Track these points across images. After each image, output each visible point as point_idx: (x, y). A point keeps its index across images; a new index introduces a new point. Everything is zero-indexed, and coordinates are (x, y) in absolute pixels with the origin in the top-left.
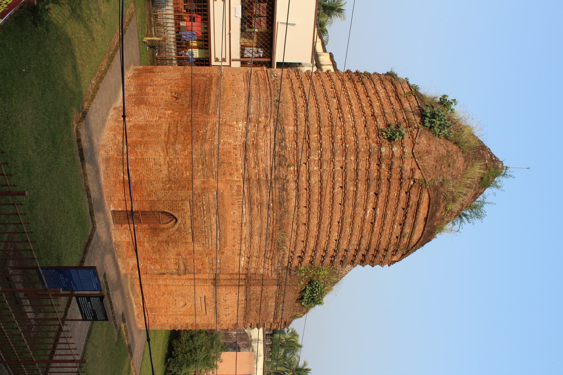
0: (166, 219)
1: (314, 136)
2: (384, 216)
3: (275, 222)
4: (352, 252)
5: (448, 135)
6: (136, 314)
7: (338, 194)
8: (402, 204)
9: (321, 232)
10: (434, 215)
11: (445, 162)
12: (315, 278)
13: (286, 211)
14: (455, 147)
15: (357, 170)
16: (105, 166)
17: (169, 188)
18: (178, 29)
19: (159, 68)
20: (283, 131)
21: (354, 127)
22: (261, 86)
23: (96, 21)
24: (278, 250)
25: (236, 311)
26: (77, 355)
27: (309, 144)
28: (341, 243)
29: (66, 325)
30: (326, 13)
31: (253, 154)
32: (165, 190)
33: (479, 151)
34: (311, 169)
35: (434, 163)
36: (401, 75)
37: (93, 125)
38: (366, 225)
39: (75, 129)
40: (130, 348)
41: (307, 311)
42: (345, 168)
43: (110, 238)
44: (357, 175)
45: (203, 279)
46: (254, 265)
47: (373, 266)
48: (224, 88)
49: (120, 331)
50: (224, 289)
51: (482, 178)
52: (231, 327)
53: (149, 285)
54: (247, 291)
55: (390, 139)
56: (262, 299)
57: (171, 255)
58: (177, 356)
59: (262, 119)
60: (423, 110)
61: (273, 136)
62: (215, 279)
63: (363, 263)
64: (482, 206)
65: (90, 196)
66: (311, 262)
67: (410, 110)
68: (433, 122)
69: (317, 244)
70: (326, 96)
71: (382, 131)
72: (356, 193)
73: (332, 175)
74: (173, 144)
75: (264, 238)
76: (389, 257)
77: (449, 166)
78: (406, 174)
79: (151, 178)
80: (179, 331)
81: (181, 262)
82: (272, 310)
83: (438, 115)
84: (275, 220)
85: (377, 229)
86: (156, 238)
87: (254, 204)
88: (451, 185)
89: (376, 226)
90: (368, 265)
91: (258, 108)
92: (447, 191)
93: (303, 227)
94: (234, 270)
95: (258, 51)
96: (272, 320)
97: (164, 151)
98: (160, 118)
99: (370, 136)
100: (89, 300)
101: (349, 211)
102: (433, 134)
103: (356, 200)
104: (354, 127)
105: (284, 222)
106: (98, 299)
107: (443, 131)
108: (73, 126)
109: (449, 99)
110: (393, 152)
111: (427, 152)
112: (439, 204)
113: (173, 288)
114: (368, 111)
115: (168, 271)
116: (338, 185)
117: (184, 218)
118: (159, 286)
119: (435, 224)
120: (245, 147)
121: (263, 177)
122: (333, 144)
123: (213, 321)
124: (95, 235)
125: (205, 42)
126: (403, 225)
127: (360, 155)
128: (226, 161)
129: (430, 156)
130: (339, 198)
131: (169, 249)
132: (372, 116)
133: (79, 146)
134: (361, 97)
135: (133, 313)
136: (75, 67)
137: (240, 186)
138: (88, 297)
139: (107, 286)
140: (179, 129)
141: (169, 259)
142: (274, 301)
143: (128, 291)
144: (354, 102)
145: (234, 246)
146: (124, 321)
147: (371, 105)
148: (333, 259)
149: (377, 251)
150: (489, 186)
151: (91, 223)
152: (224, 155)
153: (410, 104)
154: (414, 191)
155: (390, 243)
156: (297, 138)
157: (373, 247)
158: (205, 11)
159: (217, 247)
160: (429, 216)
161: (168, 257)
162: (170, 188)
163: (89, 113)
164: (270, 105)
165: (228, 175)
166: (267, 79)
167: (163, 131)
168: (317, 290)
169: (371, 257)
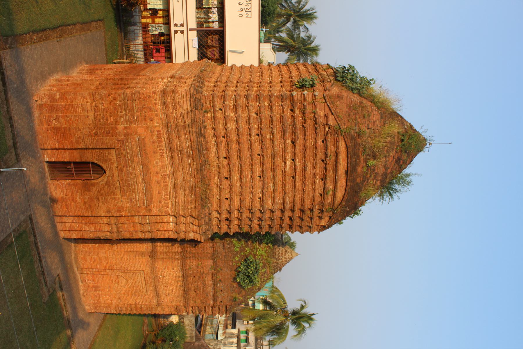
2: (304, 168)
3: (196, 173)
6: (81, 292)
7: (255, 142)
8: (320, 155)
11: (359, 112)
13: (207, 162)
14: (369, 104)
17: (95, 134)
24: (203, 207)
31: (171, 99)
35: (347, 110)
38: (287, 179)
47: (302, 233)
50: (161, 263)
65: (13, 126)
69: (241, 201)
75: (187, 192)
76: (316, 219)
77: (364, 117)
82: (210, 289)
84: (196, 170)
86: (88, 193)
87: (174, 151)
89: (297, 180)
90: (297, 232)
96: (211, 302)
97: (90, 97)
101: (269, 163)
111: (338, 97)
112: (359, 157)
113: (113, 261)
116: (254, 132)
117: (111, 169)
119: (358, 180)
123: (155, 302)
126: (324, 179)
127: (273, 99)
129: (341, 101)
130: (257, 147)
131: (100, 204)
135: (78, 290)
139: (34, 233)
142: (210, 278)
145: (160, 202)
148: (260, 222)
155: (314, 201)
160: (349, 168)
162: (96, 134)
168: (252, 265)
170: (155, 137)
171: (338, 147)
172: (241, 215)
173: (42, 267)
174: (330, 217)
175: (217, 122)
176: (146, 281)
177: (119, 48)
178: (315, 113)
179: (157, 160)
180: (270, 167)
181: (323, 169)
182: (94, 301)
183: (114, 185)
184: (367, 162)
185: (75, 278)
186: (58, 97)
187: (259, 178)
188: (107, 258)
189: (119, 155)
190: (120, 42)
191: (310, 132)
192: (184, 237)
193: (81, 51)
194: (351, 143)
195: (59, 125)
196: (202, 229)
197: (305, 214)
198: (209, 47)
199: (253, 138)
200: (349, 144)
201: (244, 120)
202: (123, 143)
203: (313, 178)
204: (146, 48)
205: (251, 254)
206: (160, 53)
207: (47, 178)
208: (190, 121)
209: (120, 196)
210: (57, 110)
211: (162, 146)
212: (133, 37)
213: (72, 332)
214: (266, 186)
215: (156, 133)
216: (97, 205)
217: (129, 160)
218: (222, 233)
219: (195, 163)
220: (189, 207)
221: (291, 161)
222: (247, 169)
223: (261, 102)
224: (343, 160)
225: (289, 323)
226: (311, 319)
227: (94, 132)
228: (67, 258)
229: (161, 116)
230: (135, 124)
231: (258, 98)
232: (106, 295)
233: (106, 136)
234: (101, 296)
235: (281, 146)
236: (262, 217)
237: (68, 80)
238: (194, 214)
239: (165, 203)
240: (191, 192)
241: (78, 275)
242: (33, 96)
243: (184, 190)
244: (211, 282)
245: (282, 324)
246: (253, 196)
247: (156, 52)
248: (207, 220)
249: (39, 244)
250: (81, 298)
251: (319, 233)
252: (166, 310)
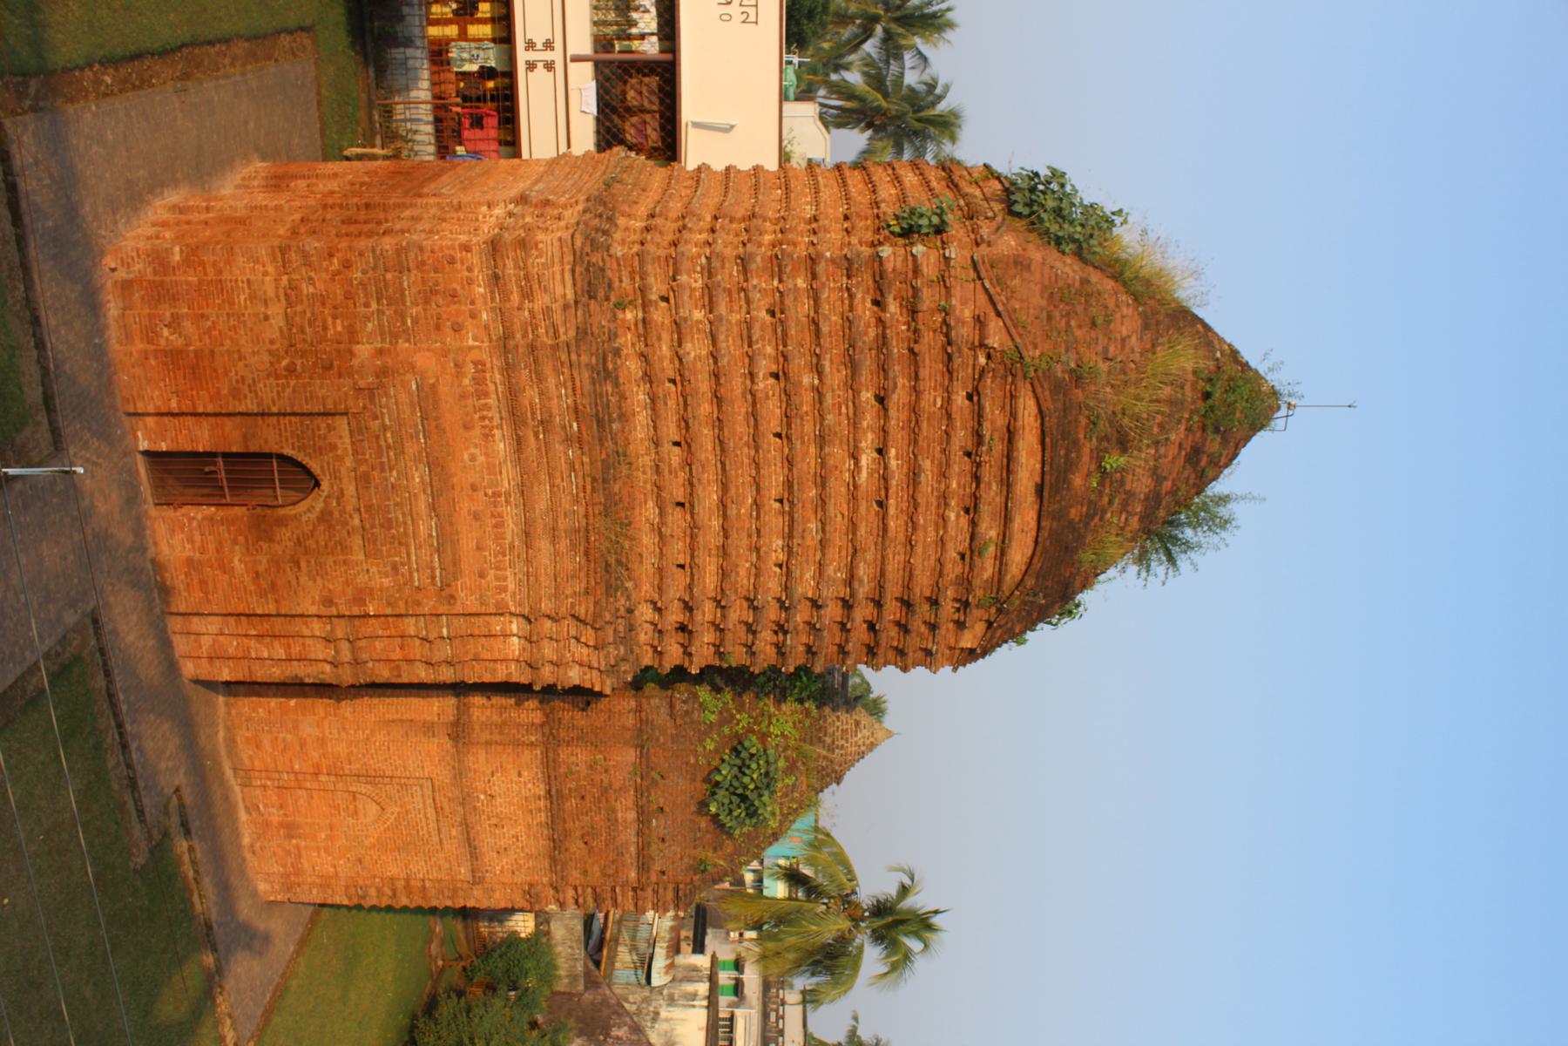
2: (914, 475)
3: (589, 487)
6: (246, 840)
8: (961, 437)
9: (734, 534)
11: (1080, 309)
16: (120, 305)
17: (287, 369)
24: (610, 590)
31: (517, 267)
32: (277, 377)
34: (683, 313)
35: (1044, 303)
38: (863, 509)
44: (818, 334)
47: (905, 669)
50: (482, 755)
69: (724, 574)
72: (819, 393)
75: (564, 544)
76: (947, 629)
77: (1094, 324)
82: (629, 837)
84: (588, 480)
86: (265, 546)
87: (525, 423)
89: (892, 511)
96: (633, 875)
97: (274, 260)
101: (808, 462)
113: (342, 749)
116: (764, 366)
117: (336, 476)
119: (1074, 513)
123: (464, 872)
126: (971, 509)
127: (821, 268)
129: (1026, 275)
130: (772, 412)
131: (304, 579)
135: (237, 835)
139: (105, 664)
142: (630, 803)
145: (482, 575)
148: (781, 637)
152: (436, 271)
155: (941, 575)
160: (1047, 478)
162: (291, 370)
165: (448, 331)
168: (754, 766)
170: (466, 381)
171: (1013, 415)
172: (724, 616)
173: (129, 766)
174: (990, 624)
175: (653, 339)
176: (438, 810)
177: (362, 115)
178: (946, 311)
179: (472, 450)
180: (812, 471)
182: (285, 866)
183: (345, 523)
184: (1100, 459)
185: (226, 798)
186: (177, 257)
187: (777, 505)
189: (360, 432)
190: (364, 96)
191: (931, 369)
192: (551, 681)
193: (246, 122)
195: (180, 342)
196: (607, 656)
197: (914, 612)
198: (630, 111)
199: (761, 385)
200: (1048, 405)
201: (735, 329)
202: (372, 397)
203: (938, 506)
204: (442, 114)
205: (753, 731)
206: (482, 127)
207: (145, 502)
208: (572, 333)
209: (361, 557)
210: (174, 298)
211: (487, 407)
212: (402, 81)
213: (218, 960)
214: (798, 528)
215: (471, 369)
216: (294, 582)
217: (389, 447)
218: (667, 667)
219: (586, 460)
220: (569, 592)
221: (875, 455)
222: (742, 477)
223: (785, 277)
224: (1031, 453)
225: (863, 939)
226: (930, 927)
227: (284, 363)
229: (485, 316)
230: (408, 340)
231: (777, 266)
232: (318, 849)
233: (321, 378)
234: (304, 853)
235: (844, 410)
236: (787, 621)
237: (208, 209)
238: (583, 611)
239: (497, 579)
240: (573, 547)
241: (237, 789)
242: (102, 254)
243: (554, 539)
244: (632, 815)
245: (843, 940)
246: (759, 558)
247: (472, 125)
248: (621, 628)
250: (244, 860)
251: (955, 670)
252: (497, 895)
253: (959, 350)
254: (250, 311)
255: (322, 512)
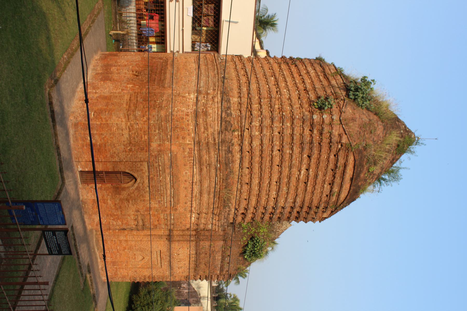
0: (127, 179)
1: (255, 106)
2: (316, 176)
3: (221, 181)
4: (288, 209)
5: (369, 106)
6: (100, 267)
7: (276, 156)
8: (331, 166)
10: (358, 176)
11: (368, 129)
12: (256, 235)
13: (232, 172)
14: (376, 117)
15: (292, 135)
17: (129, 150)
18: (139, 25)
19: (122, 53)
20: (229, 101)
21: (290, 99)
22: (210, 66)
23: (69, 5)
24: (224, 207)
25: (187, 265)
26: (47, 295)
27: (251, 112)
28: (279, 201)
29: (36, 264)
30: (261, 27)
31: (203, 120)
32: (126, 152)
33: (395, 123)
34: (253, 133)
35: (358, 129)
36: (328, 60)
37: (64, 92)
38: (300, 185)
39: (47, 92)
40: (94, 296)
41: (250, 264)
42: (282, 133)
43: (78, 195)
44: (293, 139)
45: (159, 235)
46: (203, 221)
47: (306, 222)
48: (178, 68)
49: (85, 280)
50: (177, 244)
51: (398, 146)
52: (183, 279)
53: (112, 240)
54: (197, 246)
55: (320, 108)
56: (211, 253)
57: (131, 211)
58: (136, 308)
59: (211, 91)
60: (348, 86)
61: (220, 105)
62: (169, 235)
63: (297, 219)
64: (398, 171)
65: (60, 155)
66: (252, 219)
67: (337, 86)
68: (357, 95)
69: (258, 202)
70: (265, 75)
71: (313, 101)
72: (291, 155)
73: (271, 139)
74: (133, 111)
75: (212, 195)
76: (320, 214)
77: (371, 132)
78: (335, 138)
79: (114, 141)
80: (138, 282)
81: (139, 218)
83: (360, 89)
84: (221, 180)
85: (309, 188)
86: (118, 196)
87: (203, 165)
88: (373, 149)
89: (309, 185)
90: (302, 222)
91: (207, 83)
92: (370, 155)
93: (246, 186)
94: (186, 226)
95: (206, 46)
96: (219, 272)
97: (125, 117)
98: (122, 90)
99: (303, 106)
100: (54, 234)
101: (286, 172)
102: (357, 105)
103: (292, 162)
104: (290, 99)
105: (229, 181)
106: (62, 233)
107: (365, 103)
108: (46, 89)
109: (369, 79)
110: (323, 119)
111: (352, 119)
112: (363, 166)
113: (133, 243)
114: (301, 87)
115: (128, 227)
116: (276, 148)
117: (142, 177)
118: (121, 241)
119: (360, 184)
120: (196, 115)
121: (211, 141)
122: (271, 112)
123: (168, 273)
124: (64, 190)
125: (162, 39)
126: (332, 184)
127: (295, 121)
128: (179, 126)
129: (355, 123)
130: (277, 160)
131: (130, 206)
132: (304, 90)
133: (51, 108)
134: (295, 76)
135: (98, 266)
136: (48, 38)
137: (192, 149)
138: (54, 232)
139: (74, 237)
140: (138, 99)
141: (129, 216)
143: (94, 246)
144: (289, 79)
145: (186, 203)
146: (89, 272)
147: (303, 82)
148: (272, 215)
149: (310, 208)
150: (405, 152)
151: (60, 179)
152: (177, 121)
153: (336, 82)
154: (341, 154)
155: (321, 201)
156: (241, 107)
157: (306, 204)
158: (162, 6)
159: (171, 204)
160: (354, 177)
161: (128, 213)
162: (130, 150)
163: (60, 81)
164: (217, 80)
166: (214, 61)
167: (125, 102)
168: (258, 245)
169: (304, 213)
170: (186, 153)
171: (347, 160)
172: (256, 211)
174: (332, 212)
178: (331, 134)
179: (186, 171)
181: (331, 176)
182: (112, 274)
183: (144, 190)
187: (275, 183)
188: (126, 241)
190: (114, 11)
194: (358, 156)
196: (221, 223)
201: (268, 138)
206: (153, 20)
217: (160, 170)
219: (221, 174)
222: (266, 176)
223: (284, 124)
227: (128, 148)
228: (91, 245)
229: (193, 135)
232: (123, 268)
233: (140, 152)
235: (298, 159)
238: (216, 212)
241: (98, 253)
248: (226, 215)
249: (78, 245)
250: (99, 273)
252: (177, 278)
253: (334, 144)
254: (117, 132)
255: (137, 187)
